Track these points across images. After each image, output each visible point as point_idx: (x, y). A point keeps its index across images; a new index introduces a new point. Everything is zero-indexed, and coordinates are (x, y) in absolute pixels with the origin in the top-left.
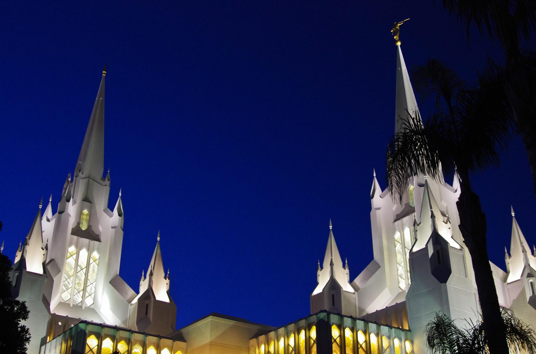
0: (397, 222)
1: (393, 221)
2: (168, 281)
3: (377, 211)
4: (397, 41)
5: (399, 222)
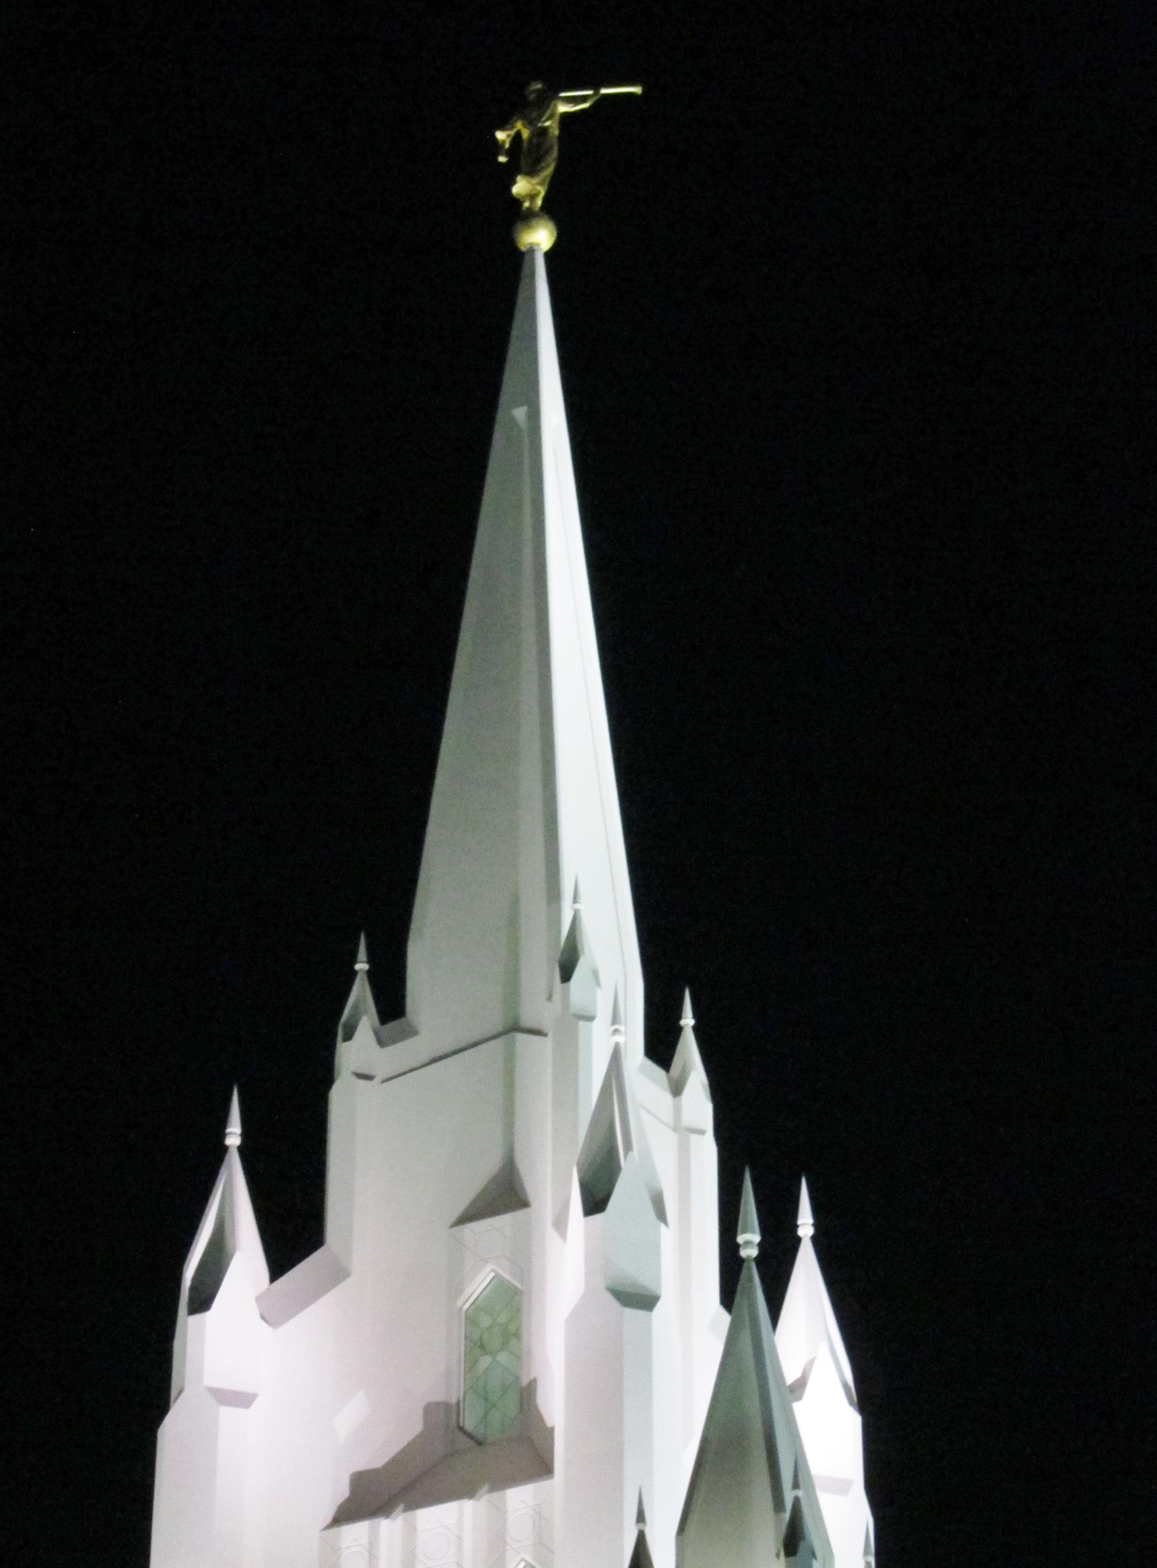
0: (357, 1532)
1: (329, 1514)
3: (228, 1415)
5: (389, 1528)
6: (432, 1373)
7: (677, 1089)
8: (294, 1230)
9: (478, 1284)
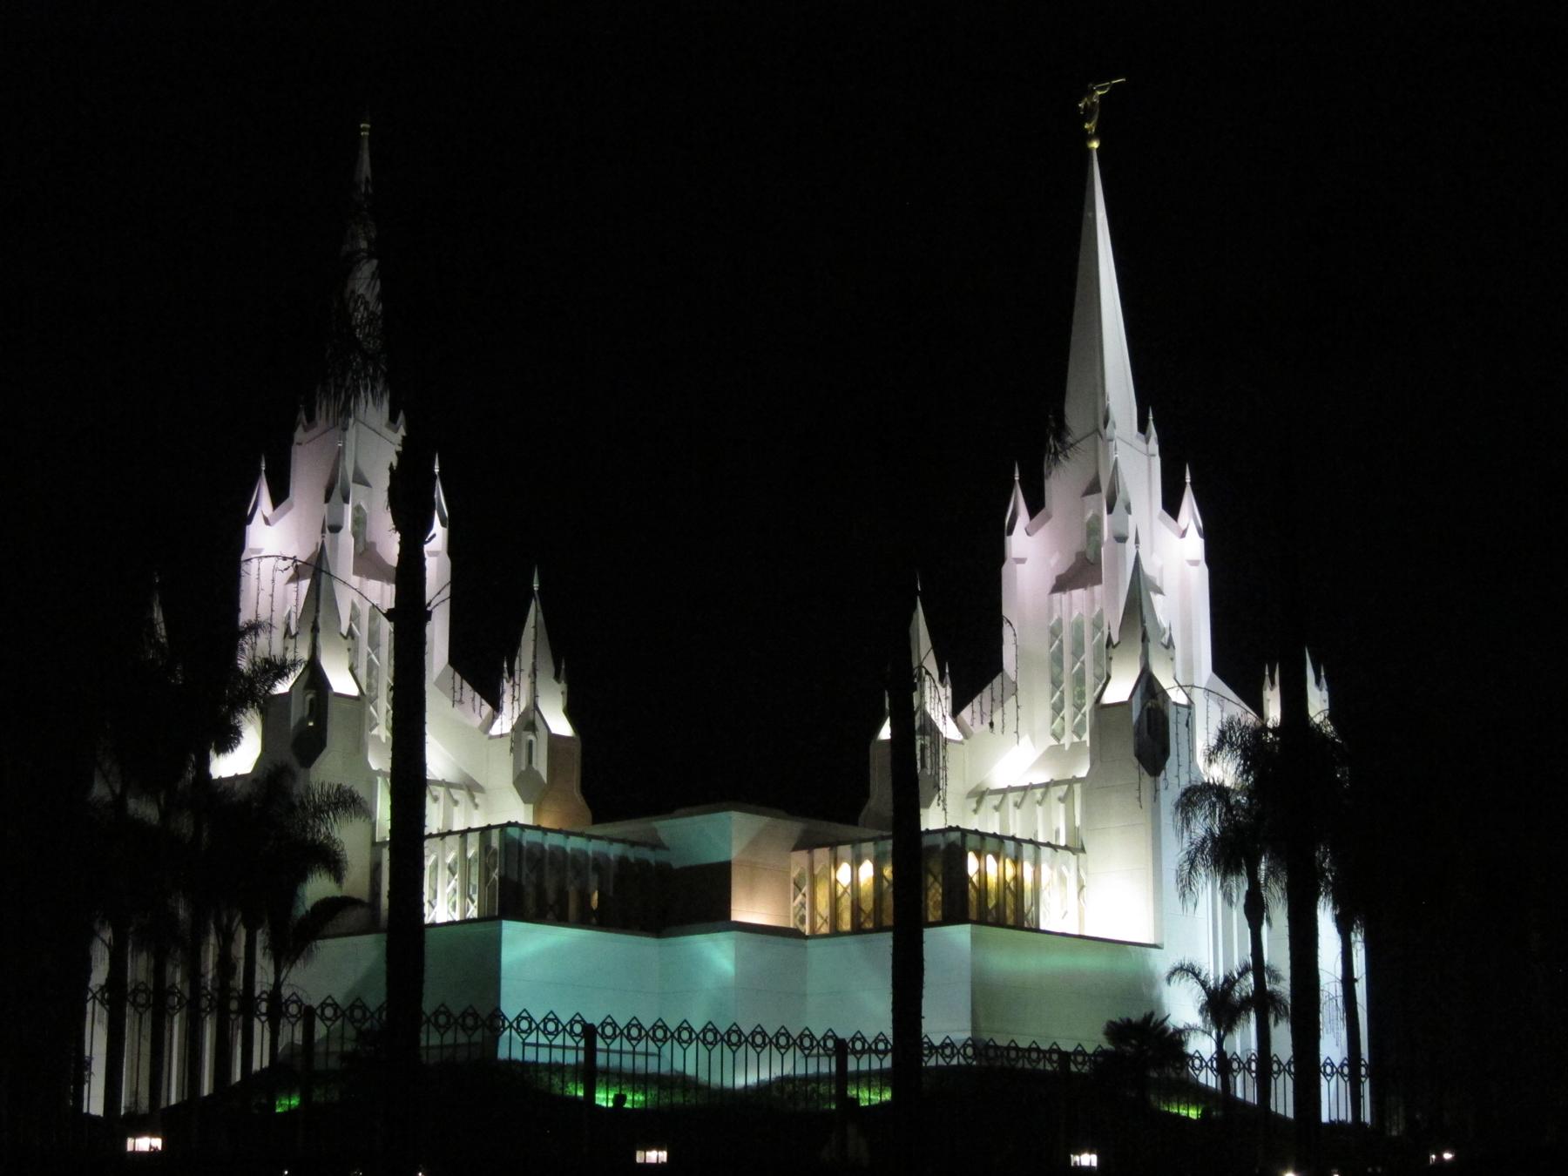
0: (1057, 596)
2: (562, 687)
4: (1091, 138)
6: (1077, 542)
7: (1147, 441)
8: (1036, 505)
9: (1089, 515)
